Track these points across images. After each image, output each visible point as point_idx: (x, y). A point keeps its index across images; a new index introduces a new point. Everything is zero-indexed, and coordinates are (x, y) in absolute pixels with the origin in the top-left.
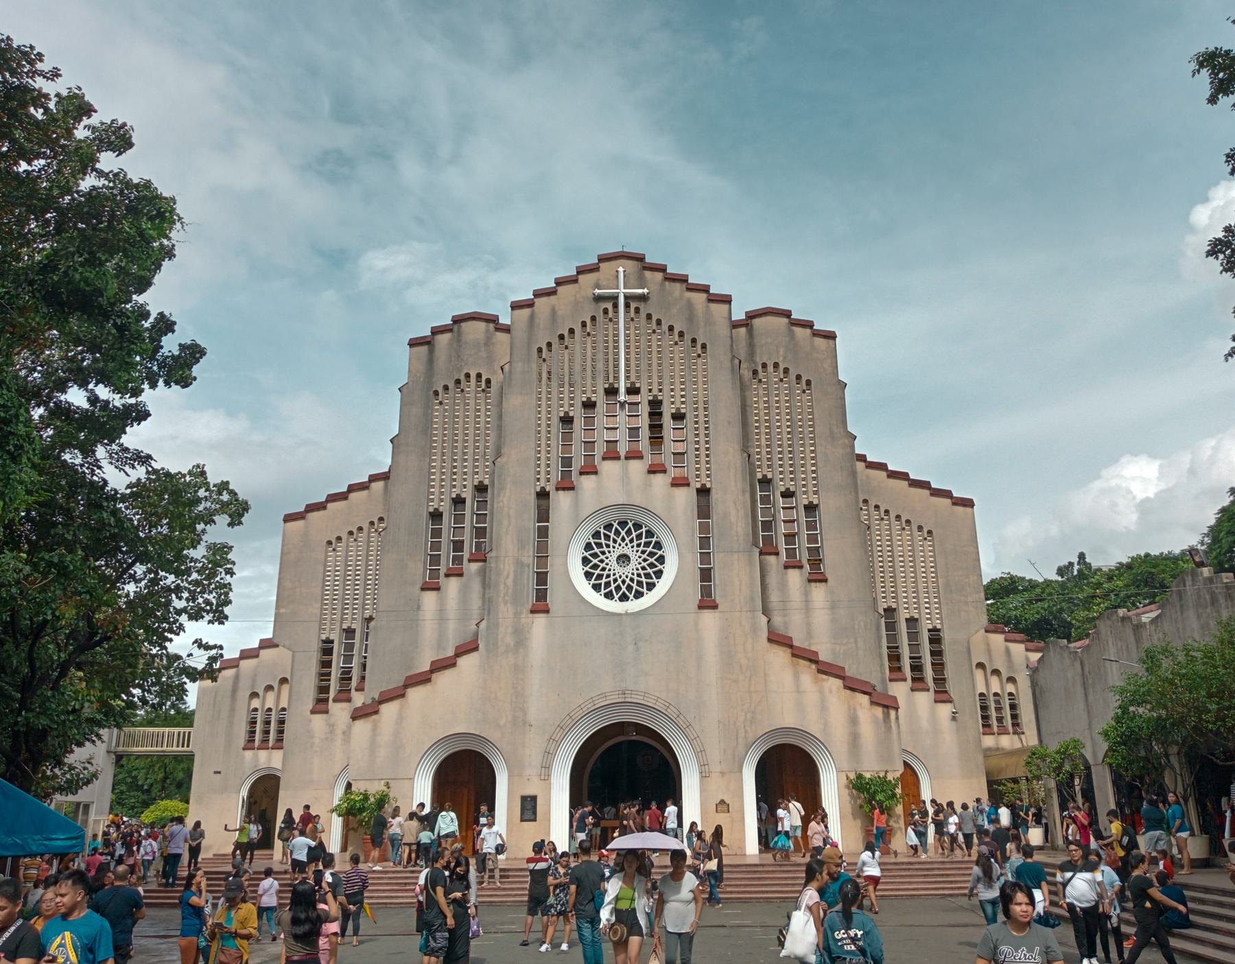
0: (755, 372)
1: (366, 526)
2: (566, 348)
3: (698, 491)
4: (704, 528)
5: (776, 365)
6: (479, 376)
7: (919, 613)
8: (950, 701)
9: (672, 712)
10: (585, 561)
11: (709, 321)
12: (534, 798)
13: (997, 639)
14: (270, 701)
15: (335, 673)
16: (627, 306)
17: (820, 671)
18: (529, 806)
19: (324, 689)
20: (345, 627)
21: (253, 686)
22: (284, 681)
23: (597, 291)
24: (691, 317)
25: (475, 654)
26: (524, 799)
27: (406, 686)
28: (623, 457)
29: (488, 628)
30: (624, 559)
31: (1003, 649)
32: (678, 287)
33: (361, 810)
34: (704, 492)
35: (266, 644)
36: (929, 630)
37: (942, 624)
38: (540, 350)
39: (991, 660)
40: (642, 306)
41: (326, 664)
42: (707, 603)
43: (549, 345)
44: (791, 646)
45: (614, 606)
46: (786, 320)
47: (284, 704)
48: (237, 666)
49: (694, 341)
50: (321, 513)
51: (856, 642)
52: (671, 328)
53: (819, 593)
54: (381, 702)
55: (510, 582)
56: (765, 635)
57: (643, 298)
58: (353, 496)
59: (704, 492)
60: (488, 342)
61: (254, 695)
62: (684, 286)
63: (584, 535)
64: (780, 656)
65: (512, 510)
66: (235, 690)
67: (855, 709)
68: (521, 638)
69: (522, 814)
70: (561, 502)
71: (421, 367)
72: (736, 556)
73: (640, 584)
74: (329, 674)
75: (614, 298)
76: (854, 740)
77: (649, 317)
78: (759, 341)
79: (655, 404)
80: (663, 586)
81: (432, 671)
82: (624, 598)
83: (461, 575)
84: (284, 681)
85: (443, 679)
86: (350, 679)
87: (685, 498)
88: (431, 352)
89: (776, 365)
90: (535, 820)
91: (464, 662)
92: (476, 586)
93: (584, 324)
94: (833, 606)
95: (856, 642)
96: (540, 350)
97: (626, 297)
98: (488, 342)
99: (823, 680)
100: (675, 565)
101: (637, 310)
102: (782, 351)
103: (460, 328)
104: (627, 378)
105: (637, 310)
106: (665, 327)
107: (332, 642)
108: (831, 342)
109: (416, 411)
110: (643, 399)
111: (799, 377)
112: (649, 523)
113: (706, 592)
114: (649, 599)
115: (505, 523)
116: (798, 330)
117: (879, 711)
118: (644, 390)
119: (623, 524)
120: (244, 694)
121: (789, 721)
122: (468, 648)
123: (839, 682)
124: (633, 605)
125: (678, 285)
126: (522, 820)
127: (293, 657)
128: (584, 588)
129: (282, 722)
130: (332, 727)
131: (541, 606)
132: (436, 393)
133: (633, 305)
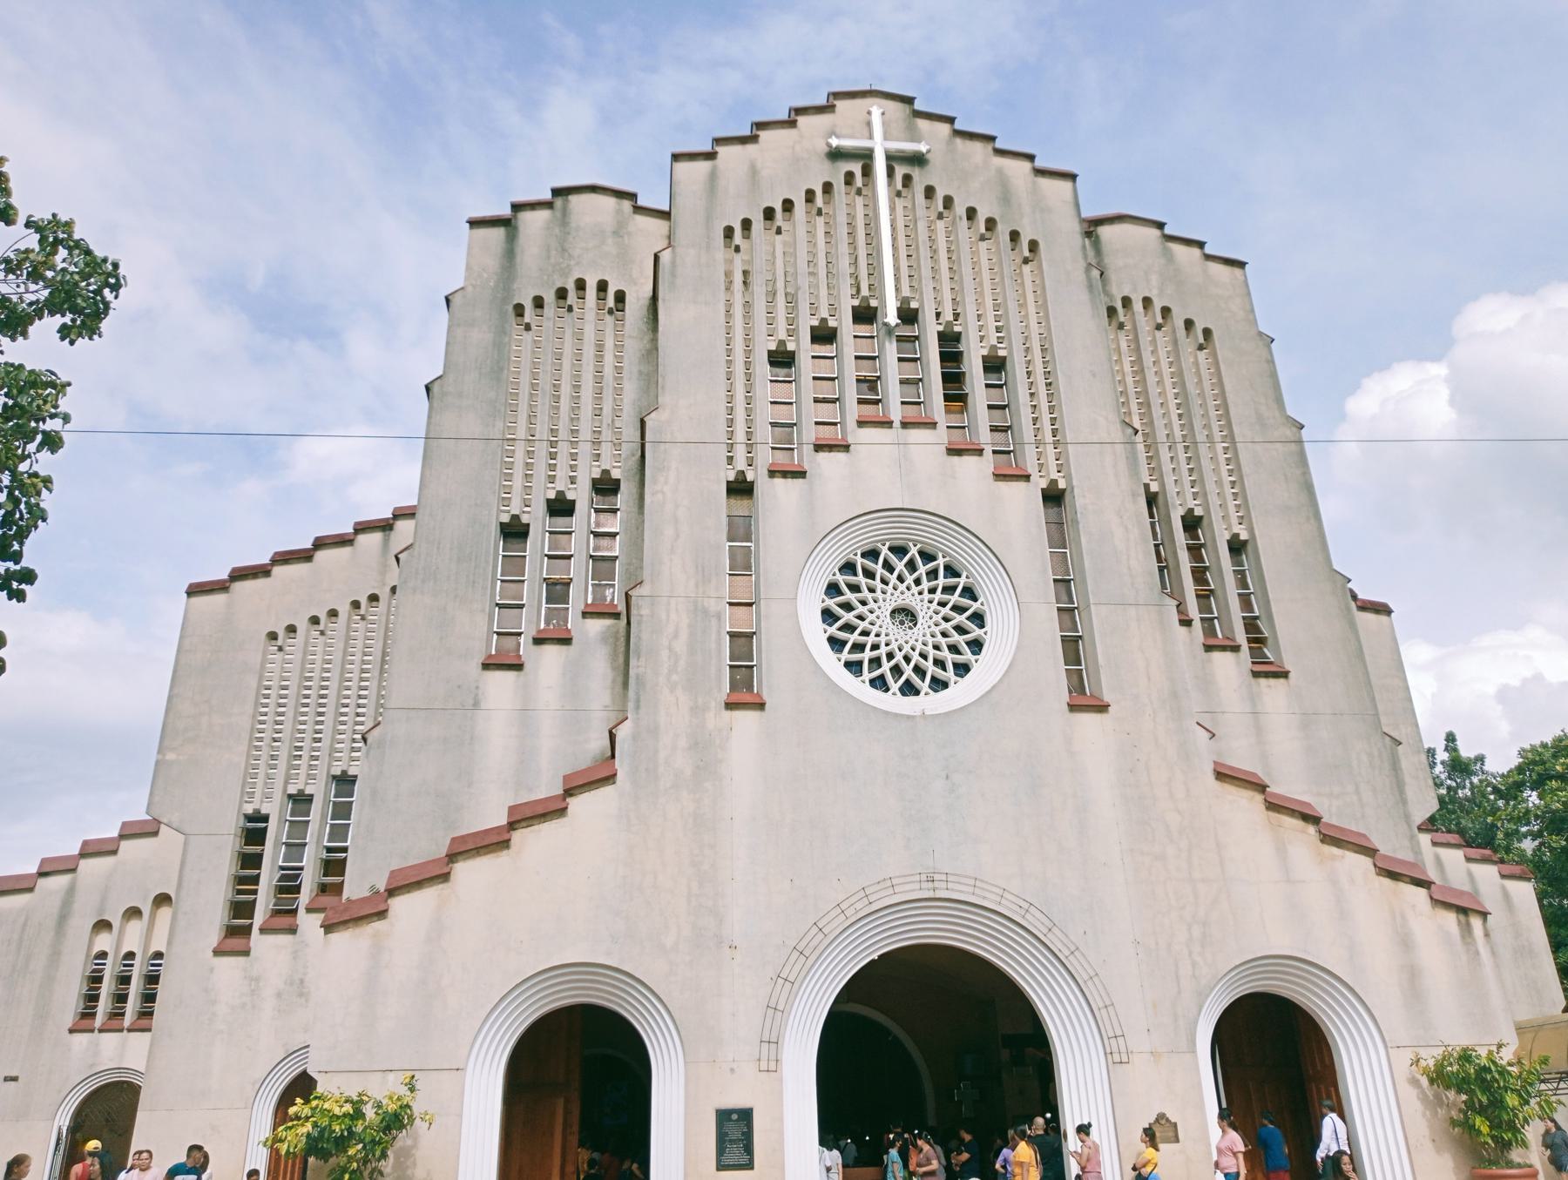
1: (344, 609)
2: (779, 231)
4: (1060, 561)
5: (1147, 302)
6: (602, 287)
9: (1035, 922)
10: (828, 616)
12: (746, 1115)
14: (133, 937)
15: (268, 877)
16: (890, 172)
18: (735, 1132)
19: (242, 909)
20: (292, 790)
21: (101, 910)
22: (163, 900)
23: (835, 142)
24: (1006, 198)
25: (606, 791)
26: (723, 1116)
27: (452, 857)
28: (897, 424)
29: (635, 737)
30: (905, 614)
32: (978, 149)
33: (342, 1143)
35: (131, 832)
38: (729, 232)
40: (916, 173)
41: (251, 861)
42: (1085, 700)
43: (747, 224)
46: (1156, 232)
47: (158, 944)
48: (73, 870)
49: (1015, 236)
50: (260, 583)
51: (1357, 791)
52: (971, 213)
54: (392, 892)
55: (681, 646)
57: (918, 160)
58: (320, 555)
59: (1053, 497)
60: (619, 231)
61: (103, 925)
63: (825, 568)
66: (63, 917)
67: (1403, 917)
68: (706, 757)
69: (721, 1151)
70: (777, 497)
71: (491, 262)
72: (1132, 611)
74: (255, 880)
75: (866, 157)
76: (1412, 977)
77: (930, 192)
78: (1113, 262)
79: (949, 340)
80: (987, 669)
81: (512, 826)
83: (566, 641)
84: (163, 900)
86: (297, 889)
88: (512, 238)
89: (1147, 302)
90: (749, 1166)
92: (600, 667)
94: (1307, 720)
95: (1357, 791)
98: (619, 231)
99: (1333, 858)
100: (1016, 627)
101: (907, 179)
102: (1154, 279)
105: (907, 179)
106: (960, 209)
107: (265, 819)
108: (1237, 271)
109: (480, 336)
110: (930, 330)
111: (1189, 324)
112: (950, 548)
113: (1077, 684)
114: (961, 692)
115: (669, 531)
116: (1177, 248)
118: (928, 316)
120: (82, 923)
121: (1281, 944)
123: (1365, 862)
125: (978, 147)
126: (721, 1167)
127: (186, 844)
130: (254, 982)
131: (744, 694)
132: (519, 310)
133: (900, 171)
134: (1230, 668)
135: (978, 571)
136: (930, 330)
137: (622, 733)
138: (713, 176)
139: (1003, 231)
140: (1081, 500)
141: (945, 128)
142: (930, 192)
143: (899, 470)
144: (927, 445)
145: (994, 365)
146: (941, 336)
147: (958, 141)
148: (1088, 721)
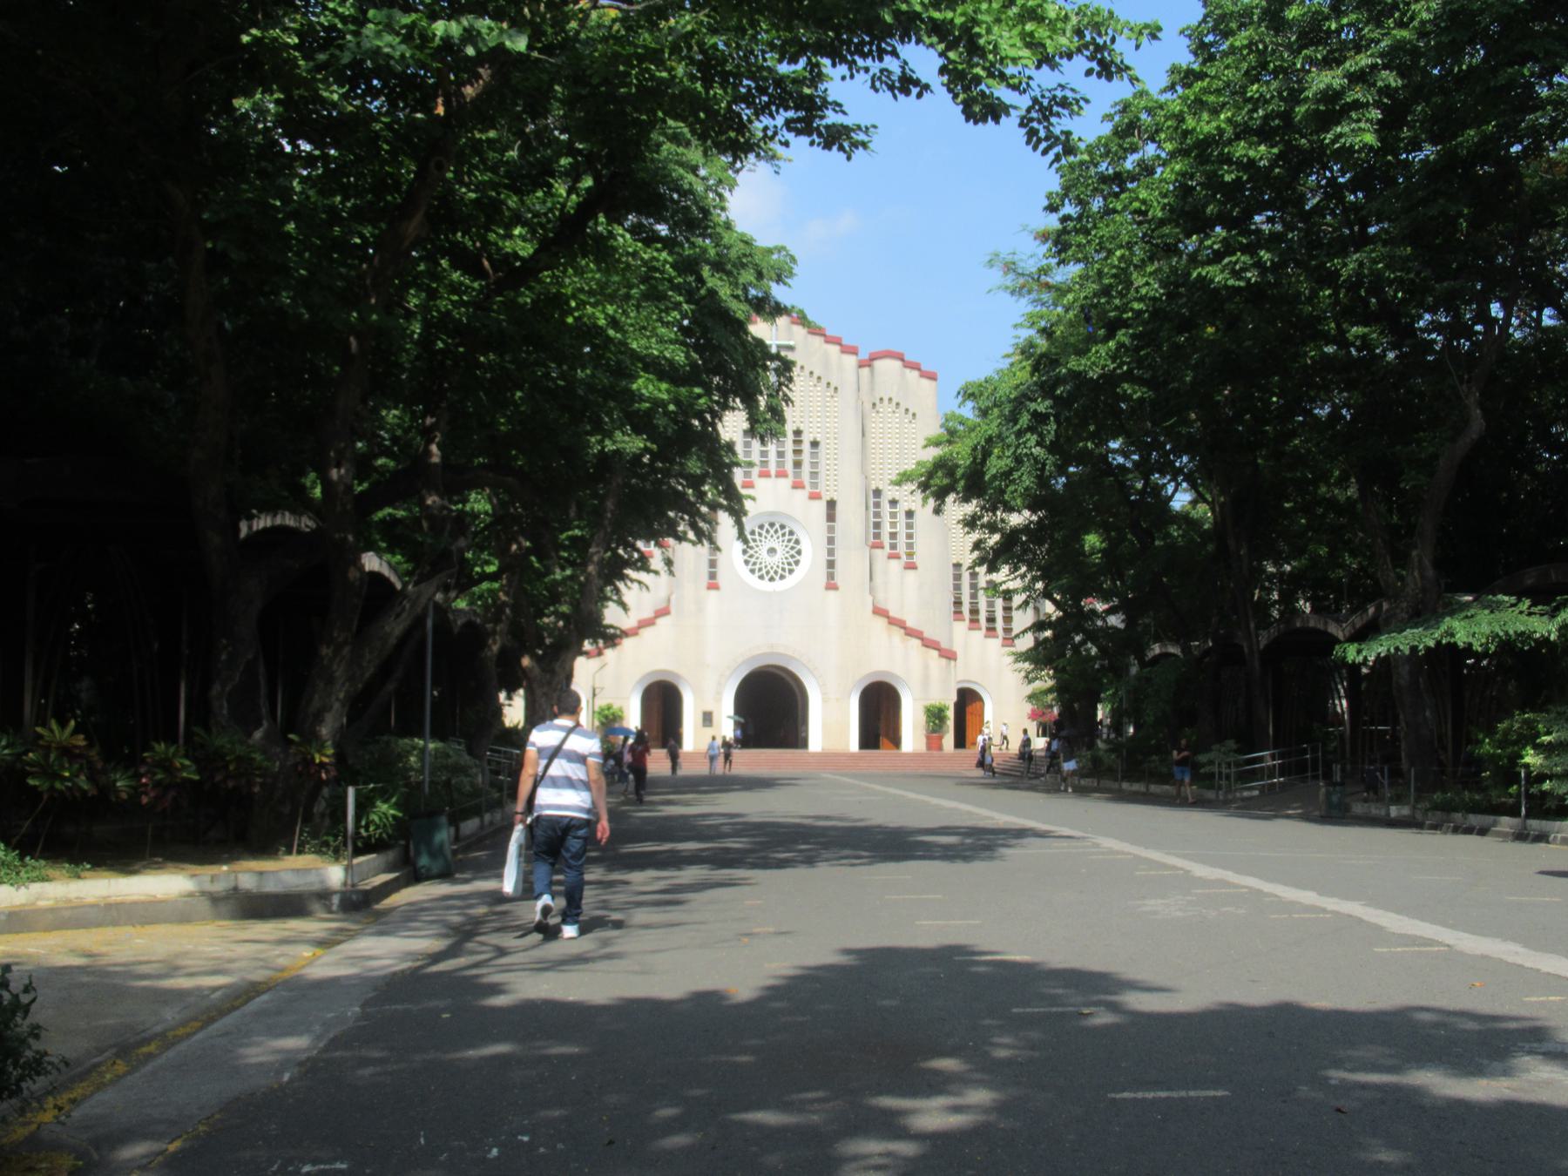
30: (772, 551)
34: (831, 504)
42: (831, 586)
45: (765, 585)
56: (870, 608)
59: (831, 504)
64: (881, 622)
76: (926, 682)
80: (800, 572)
85: (646, 633)
87: (820, 508)
91: (661, 621)
112: (790, 525)
114: (791, 581)
116: (908, 371)
117: (944, 661)
119: (772, 525)
122: (663, 612)
124: (779, 585)
135: (800, 534)
137: (673, 598)
139: (824, 382)
140: (840, 509)
144: (785, 484)
148: (832, 593)
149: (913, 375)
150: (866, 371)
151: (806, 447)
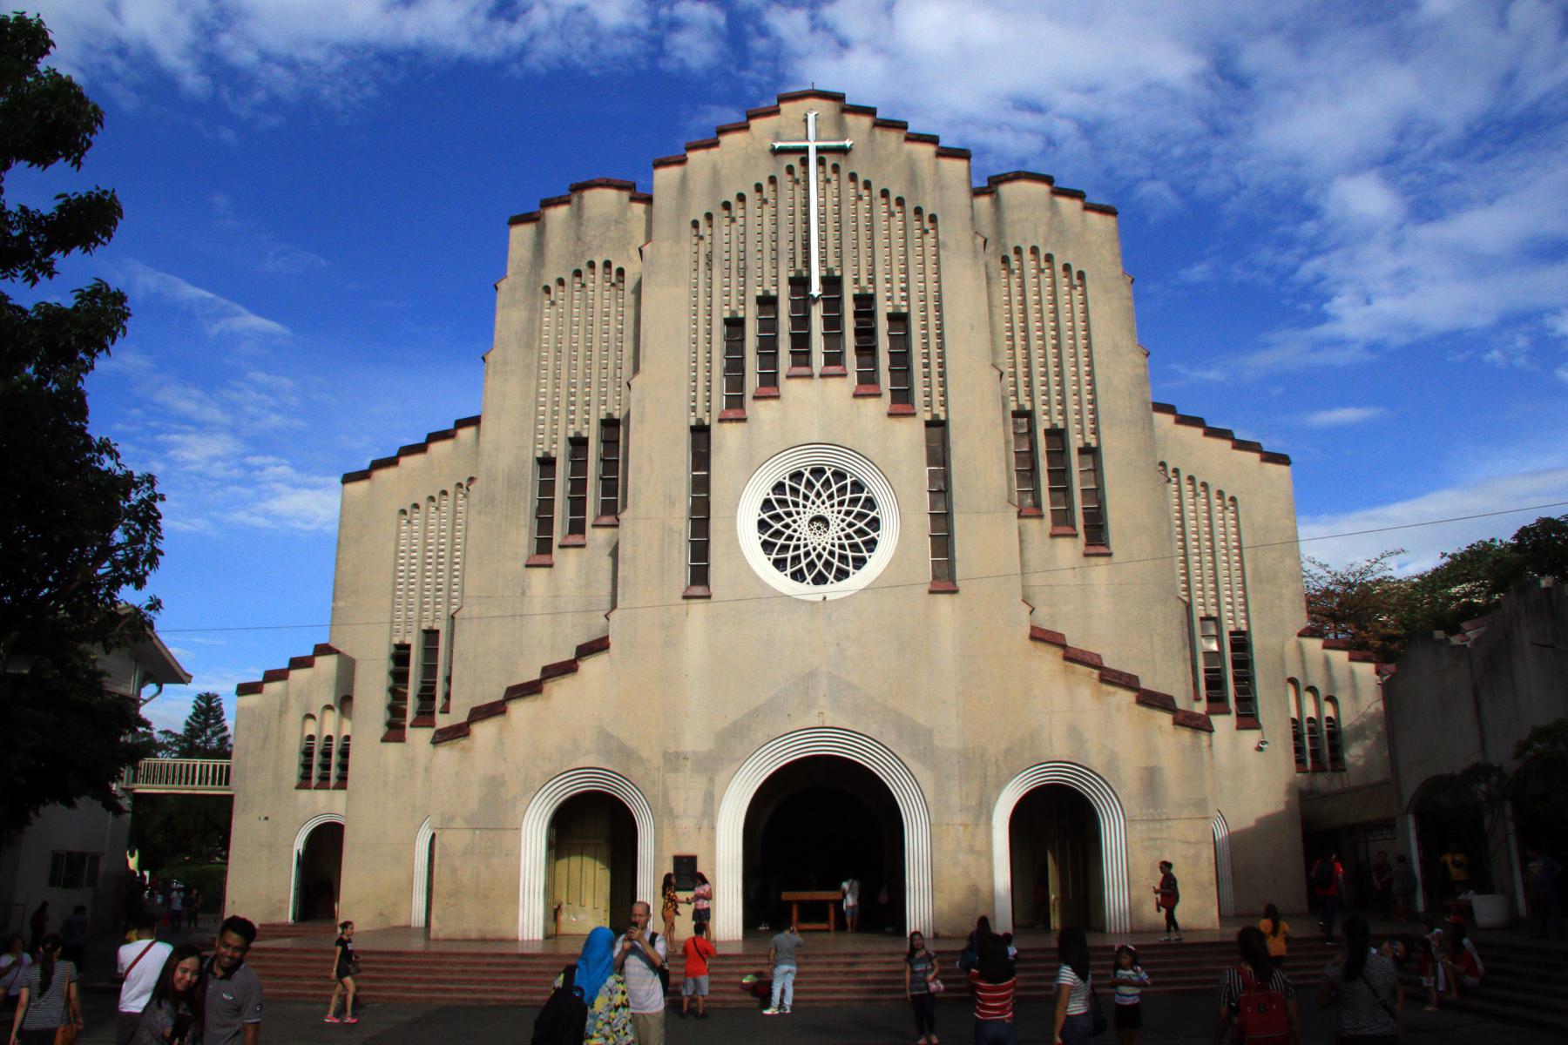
0: (1005, 260)
1: (451, 490)
3: (928, 424)
5: (1034, 250)
6: (608, 264)
7: (1219, 610)
8: (1257, 726)
11: (940, 185)
12: (692, 860)
13: (1314, 645)
16: (821, 162)
17: (1102, 679)
23: (777, 145)
24: (913, 179)
31: (1321, 660)
32: (893, 137)
36: (1232, 633)
37: (1248, 624)
39: (1305, 675)
43: (709, 216)
44: (1064, 646)
53: (1100, 571)
57: (843, 151)
59: (937, 426)
62: (903, 134)
64: (1049, 658)
65: (657, 465)
70: (726, 438)
73: (854, 547)
75: (805, 150)
78: (1011, 216)
80: (877, 562)
82: (820, 579)
85: (560, 690)
87: (910, 434)
89: (1034, 250)
91: (589, 666)
93: (759, 188)
96: (695, 224)
97: (819, 150)
99: (1109, 694)
101: (836, 168)
102: (1042, 230)
103: (581, 198)
104: (823, 262)
112: (857, 470)
114: (858, 580)
116: (1064, 202)
117: (1186, 735)
122: (598, 646)
128: (762, 564)
129: (345, 753)
134: (1069, 550)
136: (849, 291)
138: (684, 180)
141: (866, 121)
142: (853, 177)
143: (818, 411)
145: (899, 319)
146: (856, 298)
147: (878, 131)
149: (1068, 206)
150: (984, 201)
151: (882, 326)
